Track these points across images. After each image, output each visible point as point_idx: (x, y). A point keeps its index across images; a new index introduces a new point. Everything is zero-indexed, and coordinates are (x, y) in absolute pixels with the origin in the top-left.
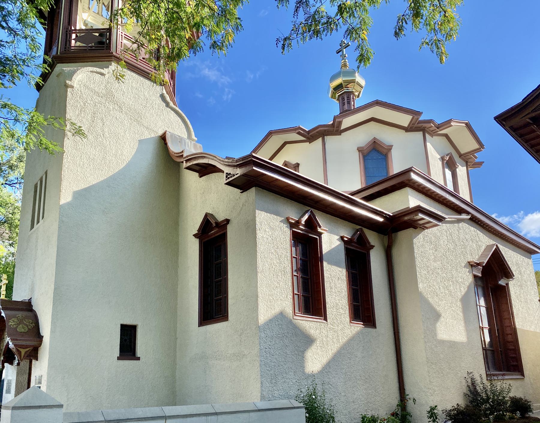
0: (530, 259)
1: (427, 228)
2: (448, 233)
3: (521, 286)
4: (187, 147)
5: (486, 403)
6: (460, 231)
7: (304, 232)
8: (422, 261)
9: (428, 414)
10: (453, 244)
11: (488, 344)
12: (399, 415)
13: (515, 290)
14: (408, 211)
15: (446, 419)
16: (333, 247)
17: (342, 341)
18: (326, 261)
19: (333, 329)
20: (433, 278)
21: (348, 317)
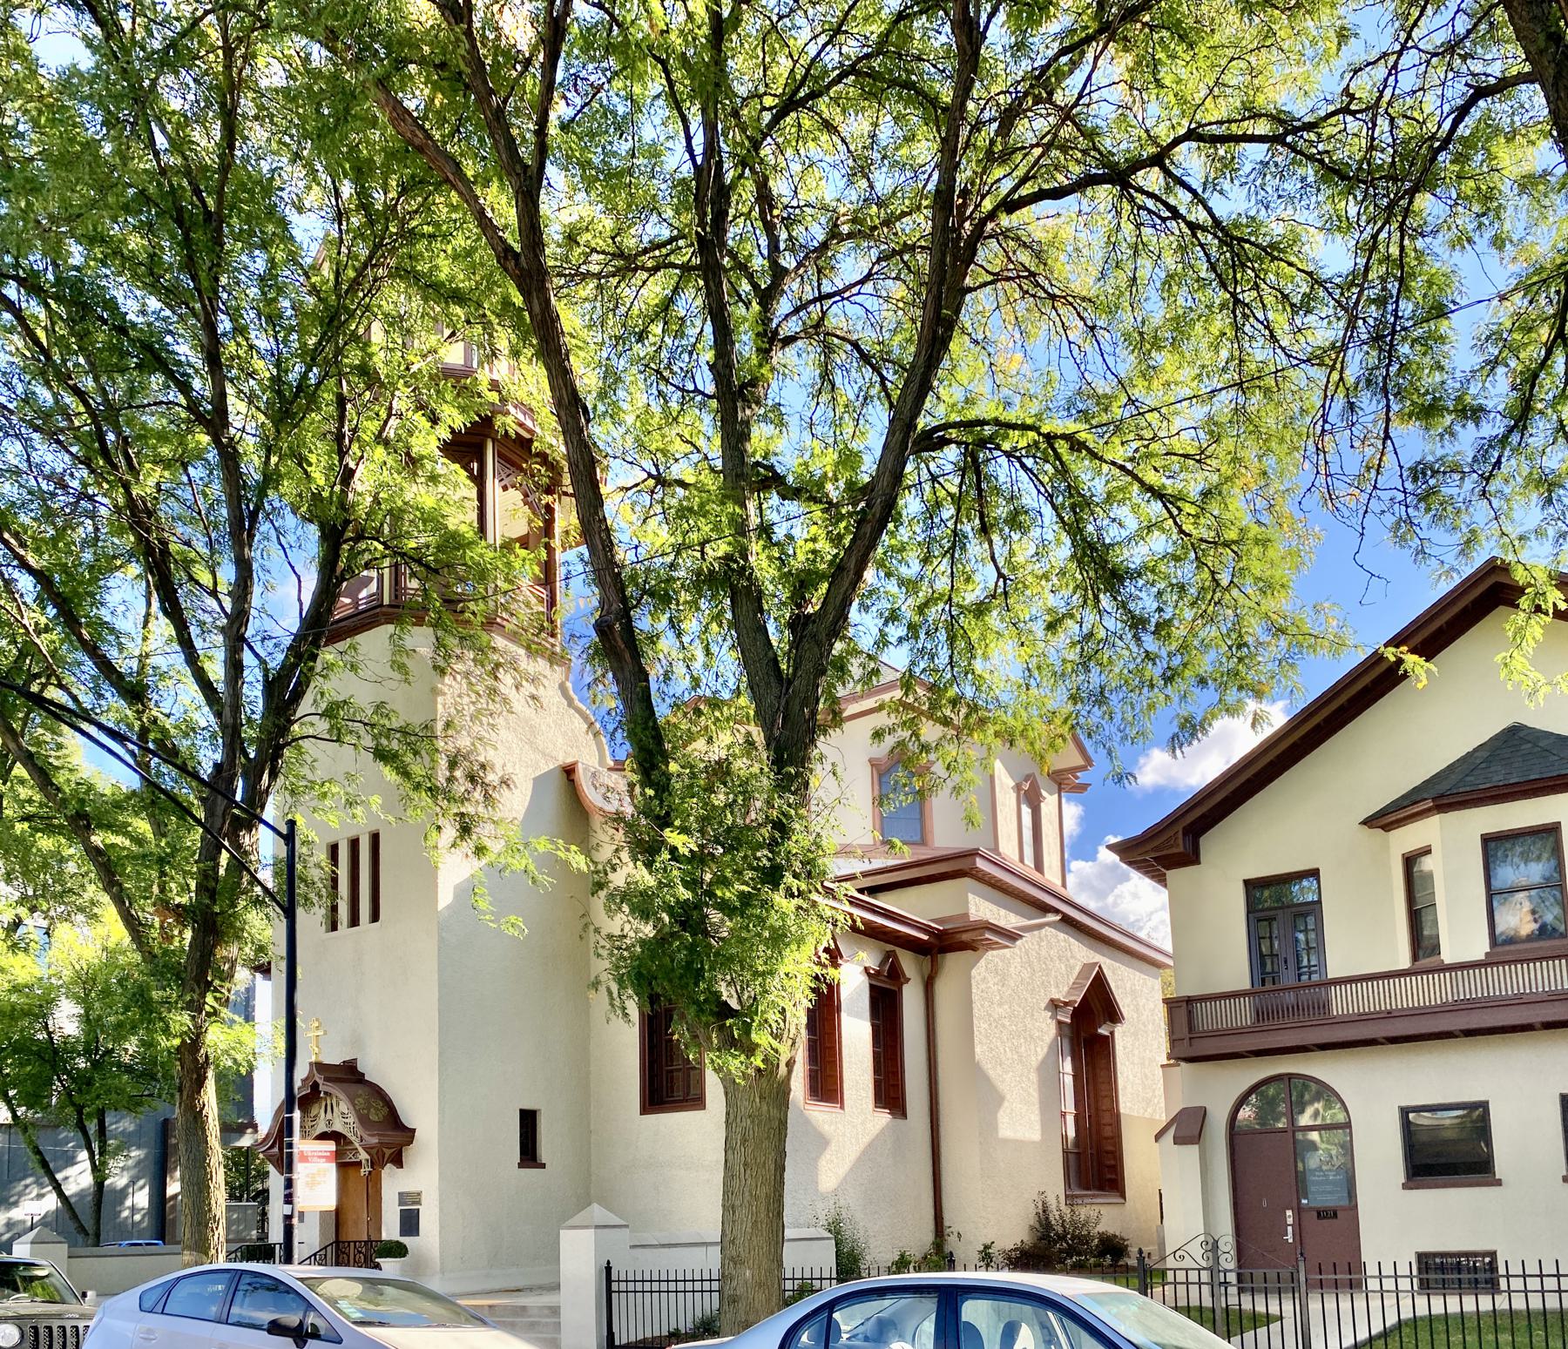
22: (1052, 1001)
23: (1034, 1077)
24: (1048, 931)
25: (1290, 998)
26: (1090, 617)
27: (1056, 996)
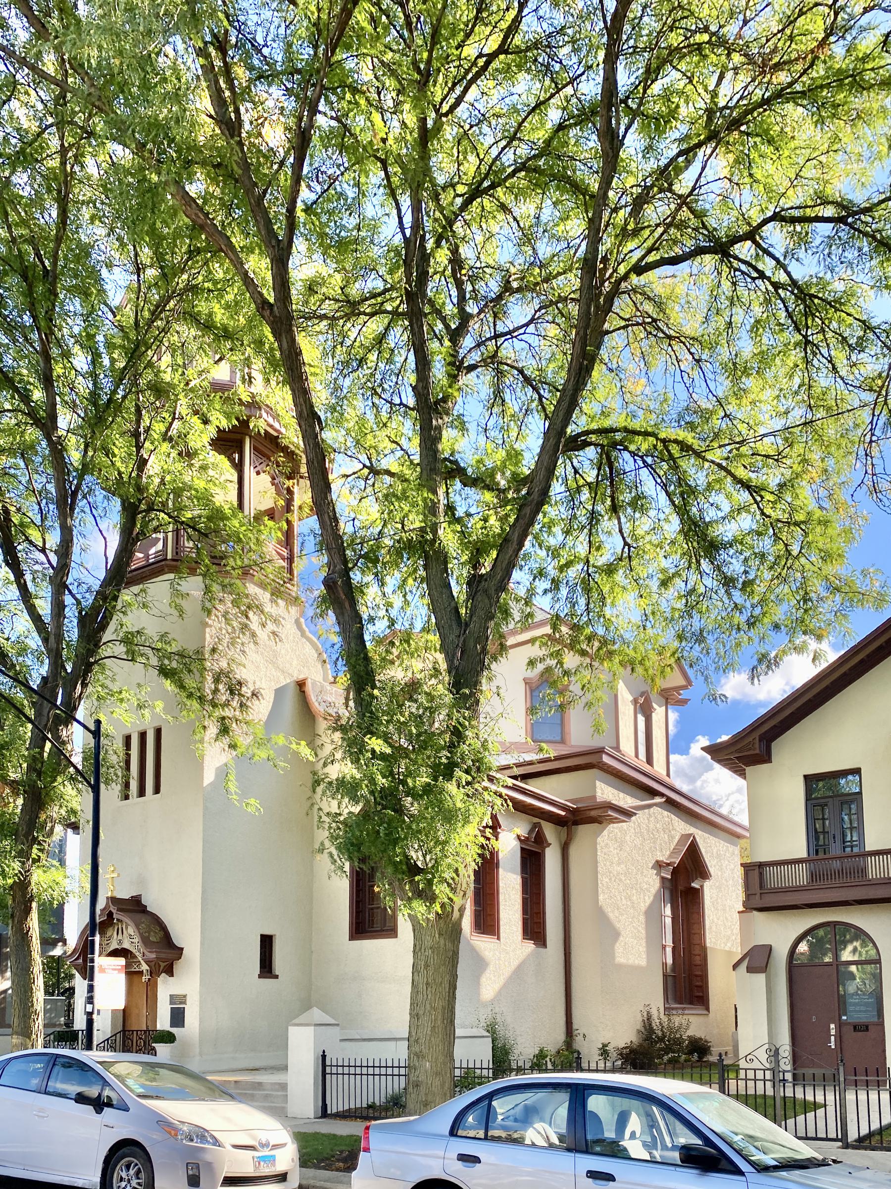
23: (642, 918)
24: (656, 810)
25: (836, 865)
26: (693, 577)
27: (661, 859)
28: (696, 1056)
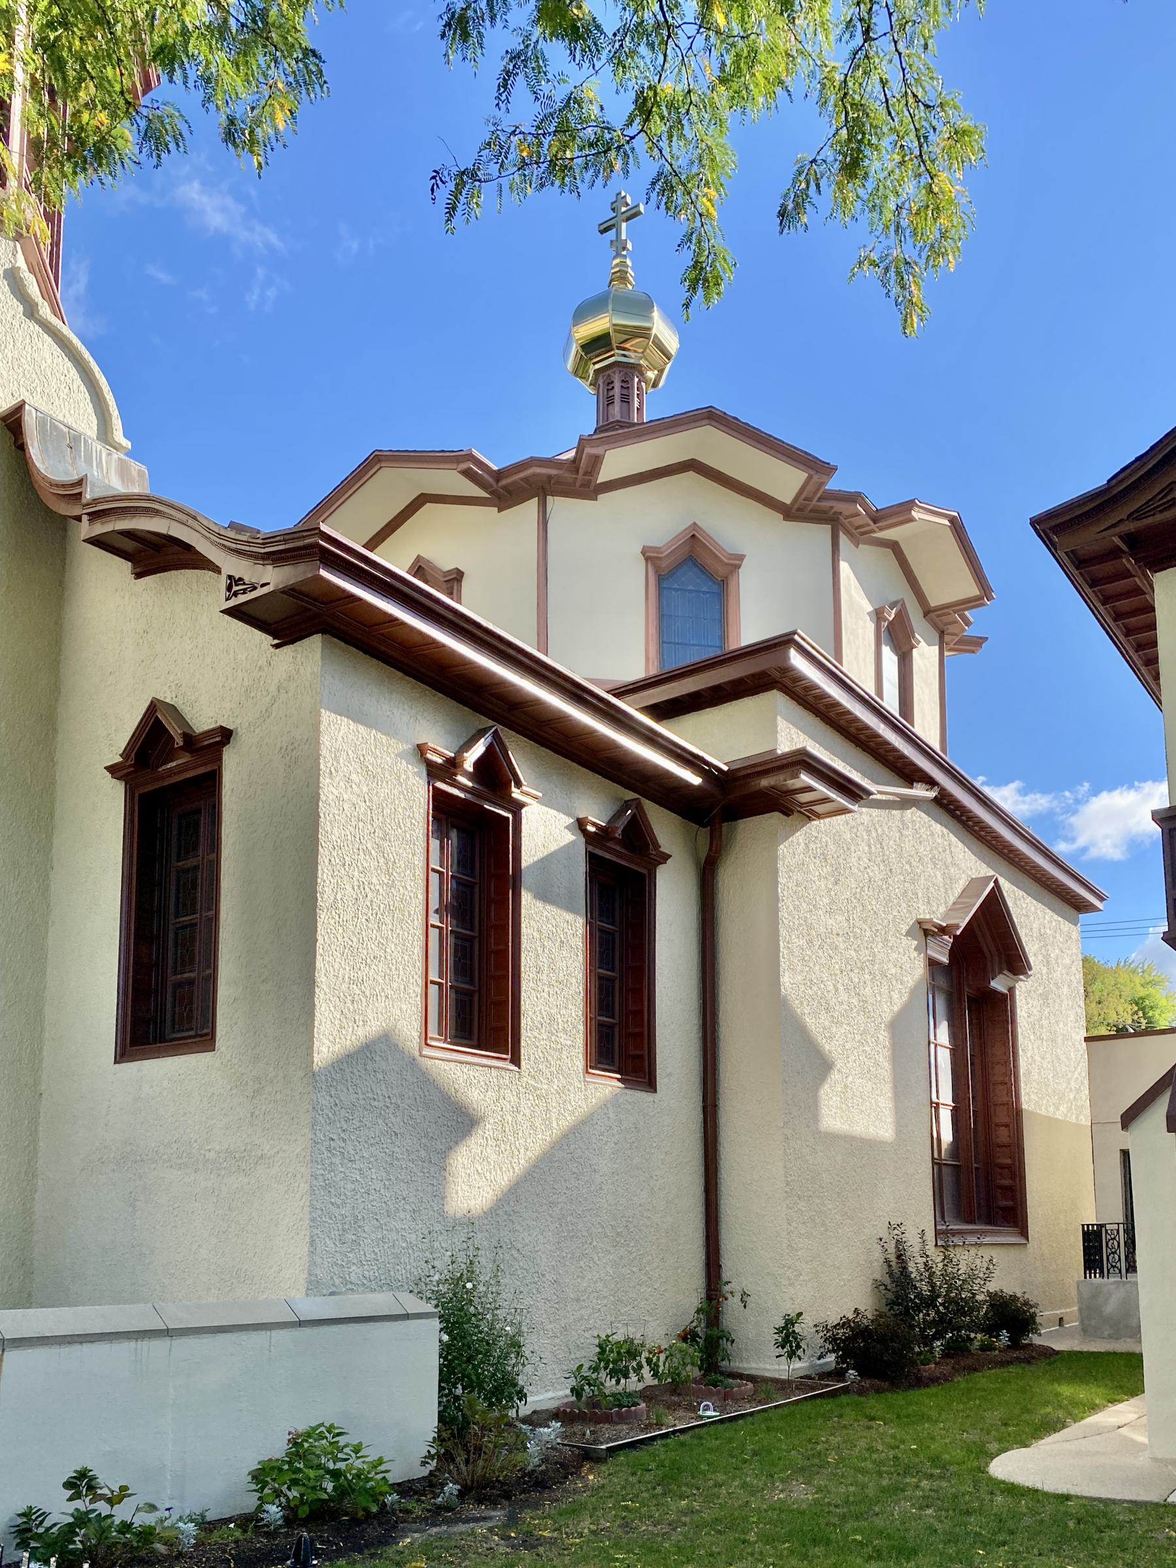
0: (1076, 925)
1: (819, 816)
2: (874, 835)
3: (1045, 997)
4: (95, 468)
5: (928, 1306)
6: (905, 832)
7: (469, 796)
8: (797, 908)
9: (776, 1336)
10: (882, 867)
11: (946, 1150)
12: (700, 1338)
13: (1030, 1006)
14: (771, 761)
15: (822, 1350)
16: (552, 850)
17: (558, 1125)
18: (529, 890)
19: (536, 1089)
20: (820, 958)
21: (581, 1056)
22: (920, 922)
23: (884, 1036)
28: (1004, 1336)
